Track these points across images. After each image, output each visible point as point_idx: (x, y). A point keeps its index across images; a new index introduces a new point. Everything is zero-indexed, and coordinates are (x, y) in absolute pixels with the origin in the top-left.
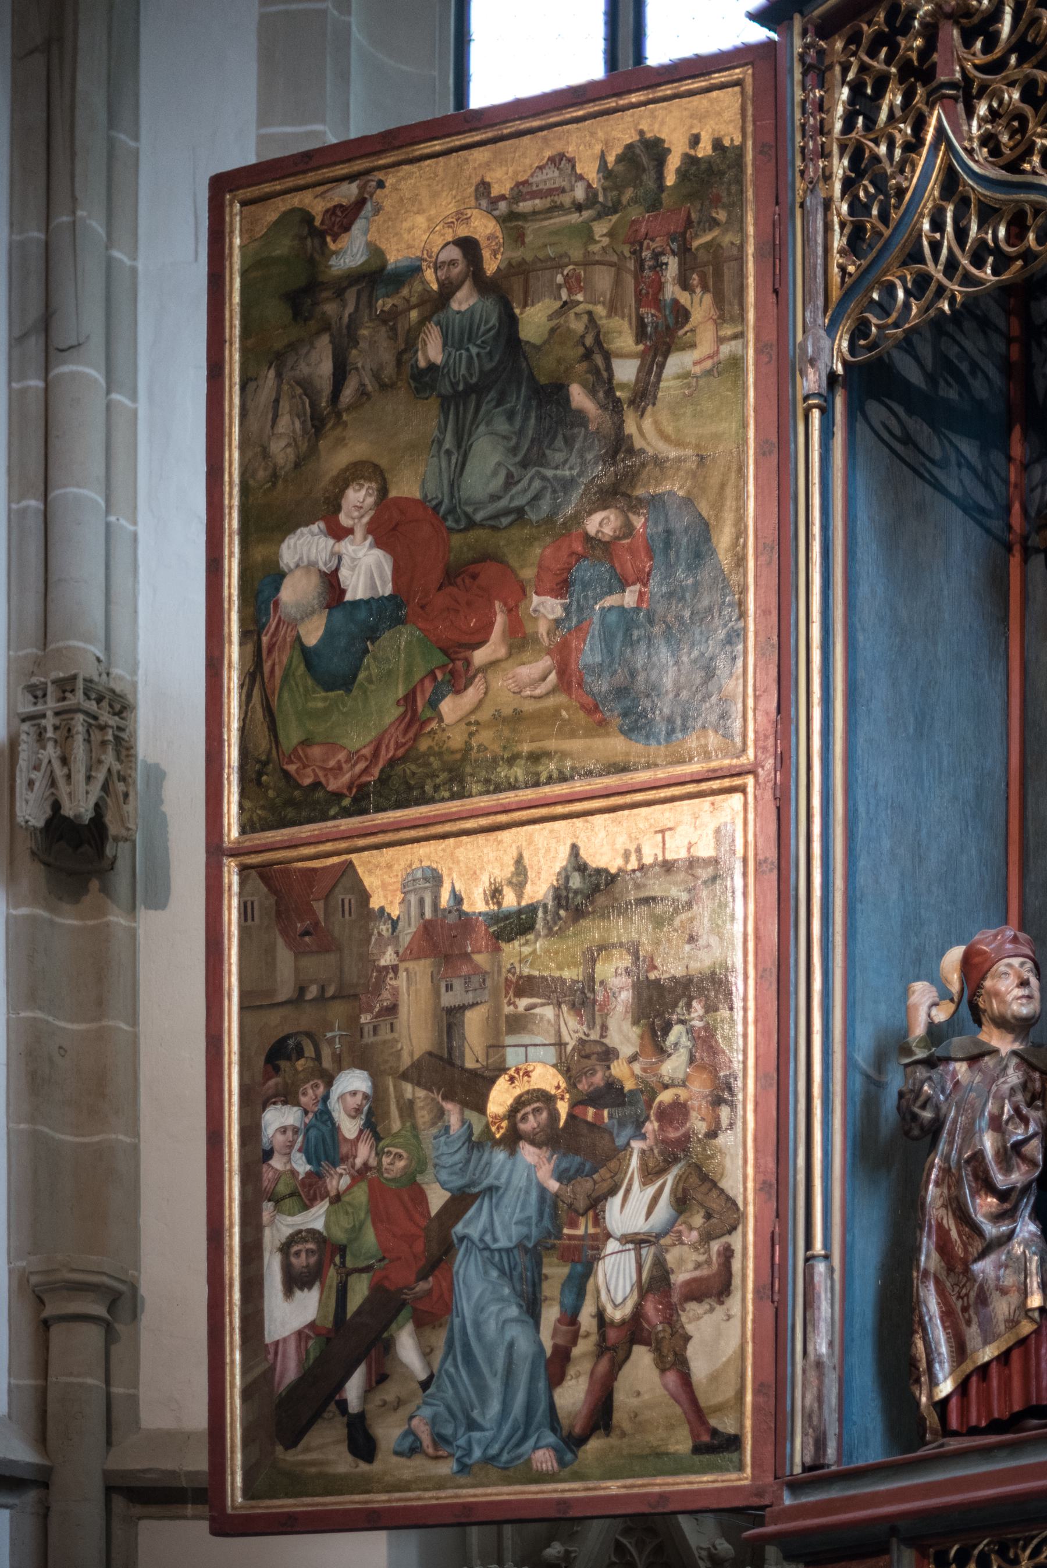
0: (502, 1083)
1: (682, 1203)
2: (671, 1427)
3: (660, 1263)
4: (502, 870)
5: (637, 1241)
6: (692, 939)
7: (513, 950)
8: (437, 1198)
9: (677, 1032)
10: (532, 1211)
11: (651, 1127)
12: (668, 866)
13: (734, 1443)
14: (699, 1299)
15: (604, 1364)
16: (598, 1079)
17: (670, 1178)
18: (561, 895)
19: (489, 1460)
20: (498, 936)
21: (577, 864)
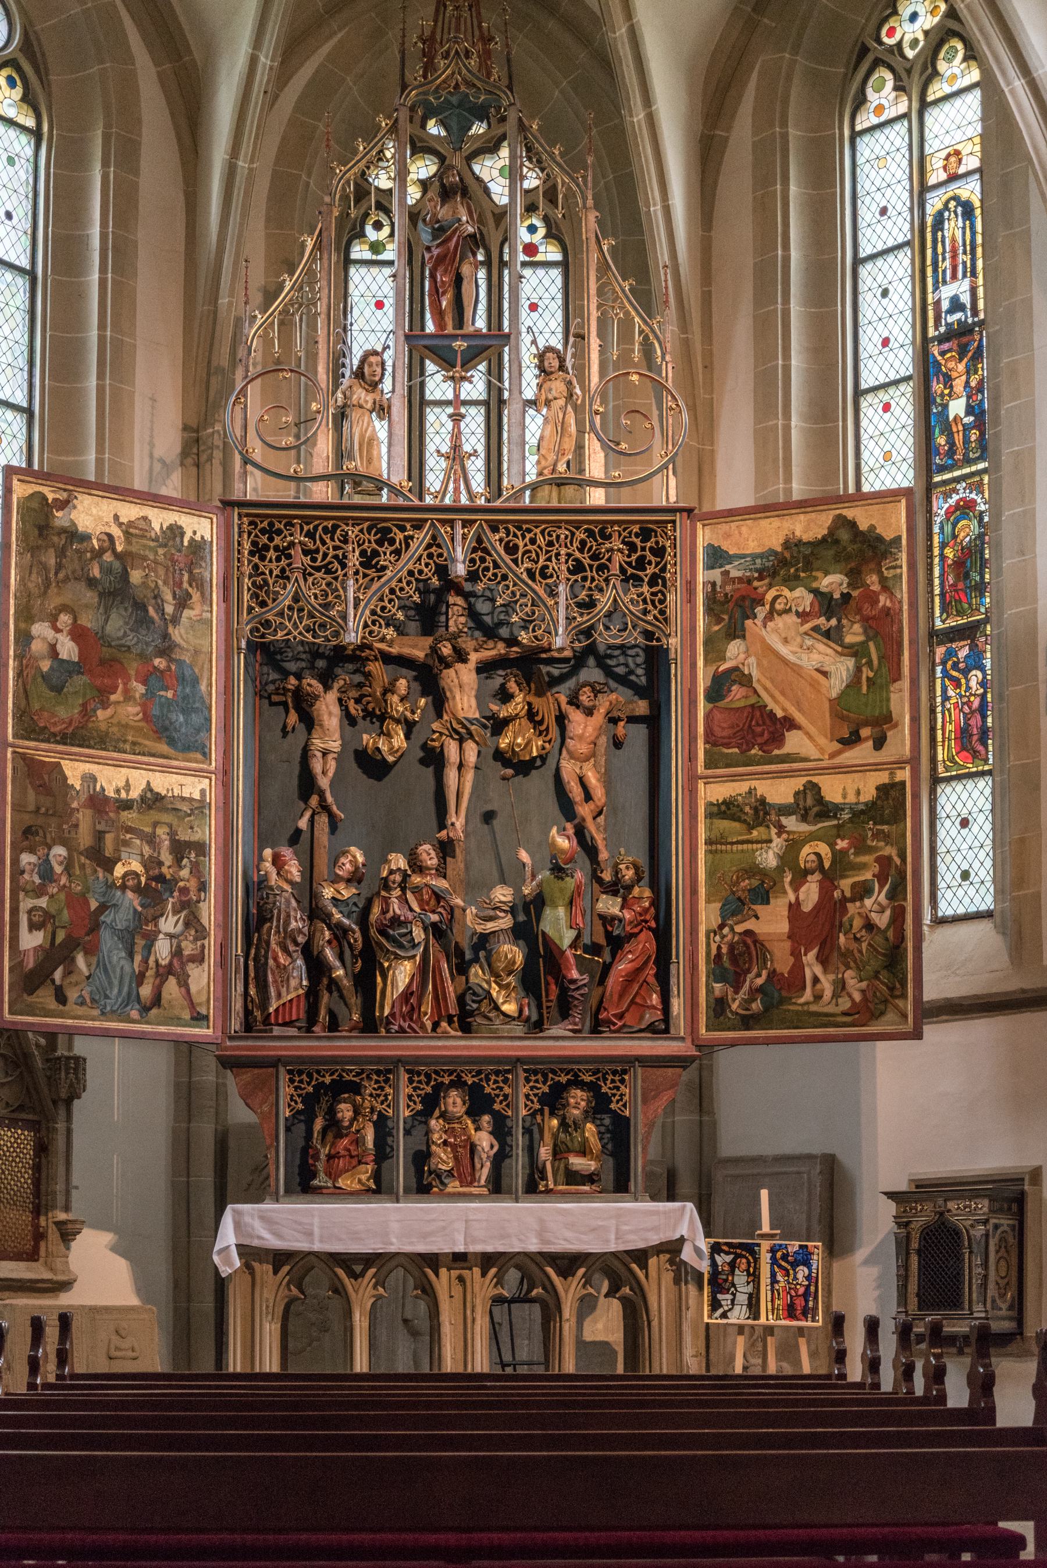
0: (119, 864)
1: (187, 925)
2: (182, 1009)
3: (179, 946)
4: (121, 784)
5: (171, 936)
6: (192, 828)
7: (125, 815)
8: (94, 905)
9: (185, 861)
10: (131, 917)
11: (176, 894)
12: (183, 799)
13: (206, 1018)
14: (193, 962)
15: (158, 981)
16: (157, 871)
17: (183, 914)
18: (143, 798)
19: (113, 1012)
20: (118, 808)
21: (149, 788)
